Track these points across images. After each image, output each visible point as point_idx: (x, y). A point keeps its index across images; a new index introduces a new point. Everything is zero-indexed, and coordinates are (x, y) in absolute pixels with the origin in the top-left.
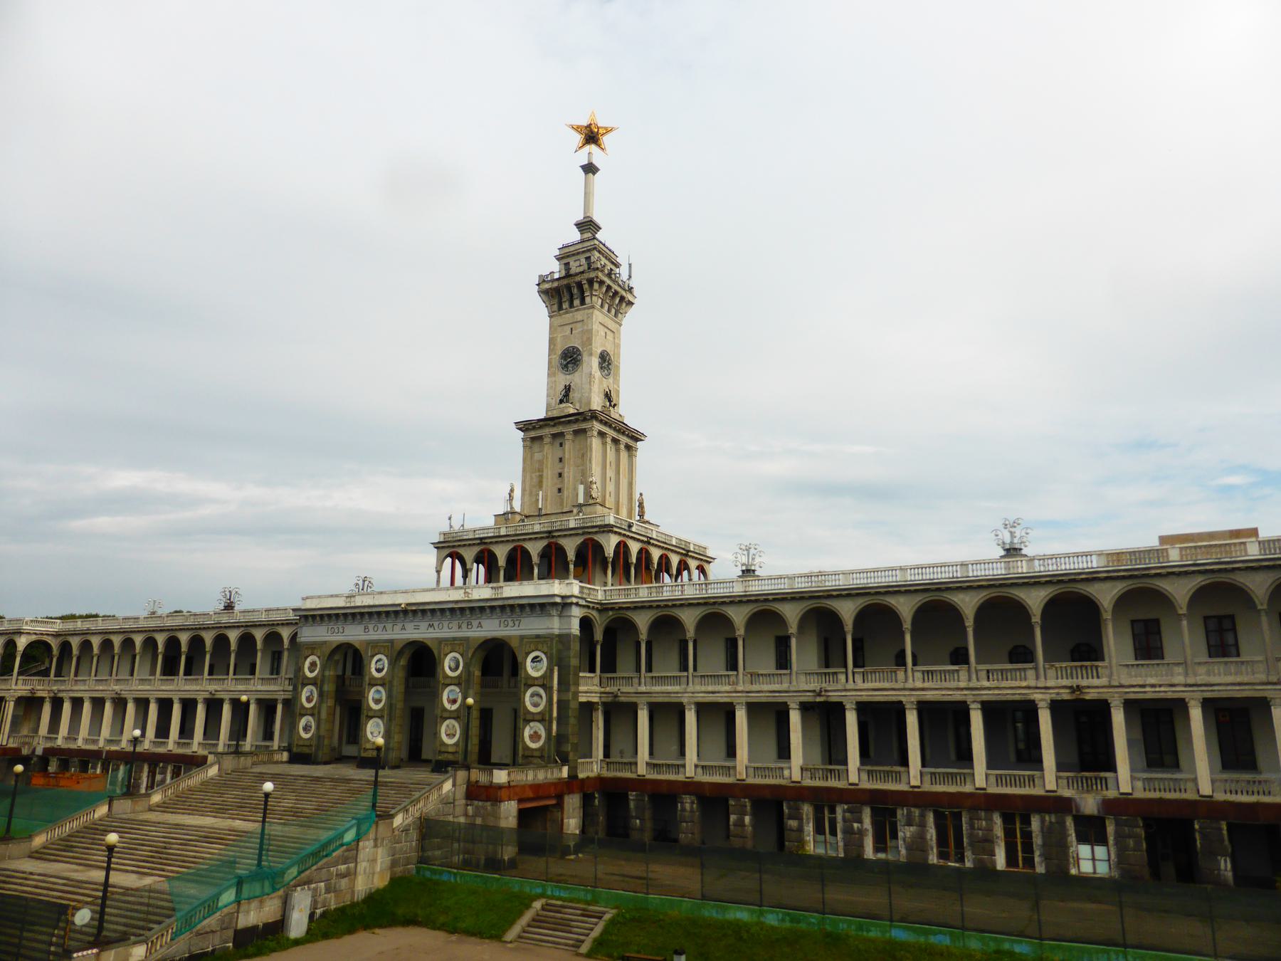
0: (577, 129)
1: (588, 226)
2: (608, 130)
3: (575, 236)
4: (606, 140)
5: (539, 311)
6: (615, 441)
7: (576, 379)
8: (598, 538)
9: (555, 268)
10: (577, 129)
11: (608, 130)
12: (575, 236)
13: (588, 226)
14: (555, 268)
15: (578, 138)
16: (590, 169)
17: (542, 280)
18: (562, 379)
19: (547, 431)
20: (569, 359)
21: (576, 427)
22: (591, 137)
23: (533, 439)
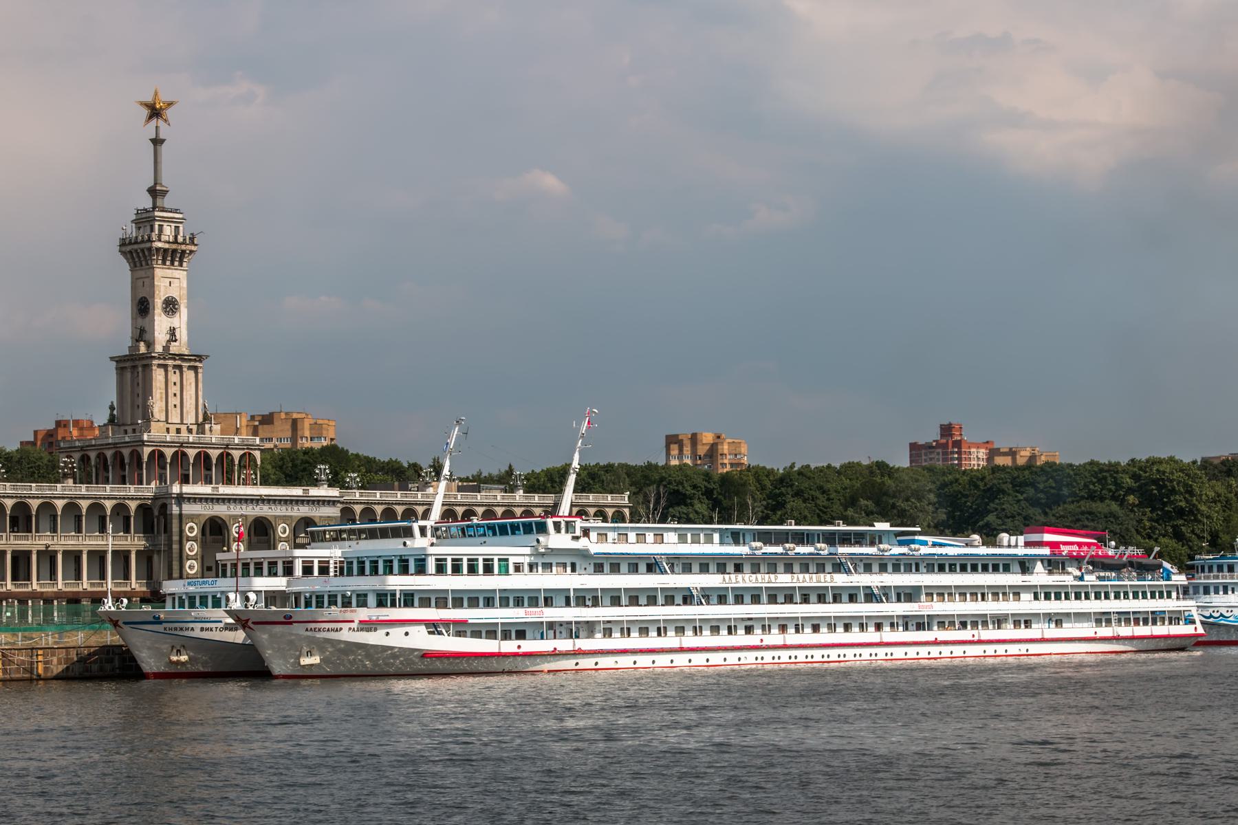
0: (147, 105)
2: (170, 104)
3: (147, 202)
4: (169, 113)
5: (124, 266)
6: (180, 367)
8: (138, 449)
9: (131, 231)
10: (147, 105)
11: (170, 104)
12: (147, 202)
15: (145, 112)
16: (157, 142)
17: (123, 243)
18: (140, 322)
19: (128, 364)
21: (145, 362)
22: (155, 112)
23: (122, 368)
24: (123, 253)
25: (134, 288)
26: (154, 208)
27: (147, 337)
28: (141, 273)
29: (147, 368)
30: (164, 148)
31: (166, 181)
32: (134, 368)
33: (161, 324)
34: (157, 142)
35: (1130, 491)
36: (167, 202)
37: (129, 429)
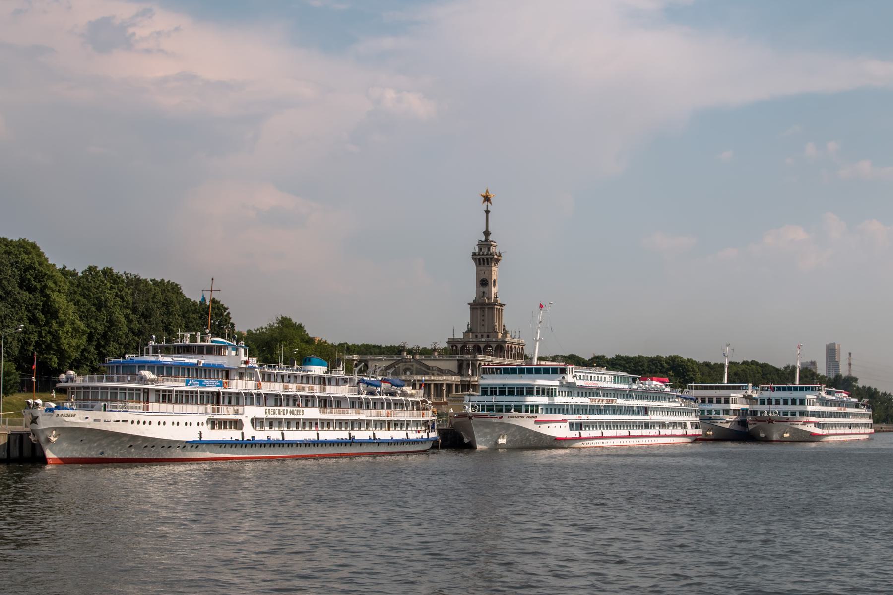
1: (487, 233)
3: (483, 238)
7: (486, 289)
13: (487, 233)
14: (477, 250)
16: (487, 212)
17: (474, 254)
18: (482, 289)
20: (484, 283)
22: (487, 199)
24: (475, 259)
25: (478, 274)
26: (486, 240)
27: (486, 295)
28: (482, 268)
29: (492, 309)
30: (490, 214)
31: (490, 230)
32: (484, 308)
33: (494, 290)
34: (487, 212)
35: (668, 370)
36: (491, 238)
37: (479, 335)
